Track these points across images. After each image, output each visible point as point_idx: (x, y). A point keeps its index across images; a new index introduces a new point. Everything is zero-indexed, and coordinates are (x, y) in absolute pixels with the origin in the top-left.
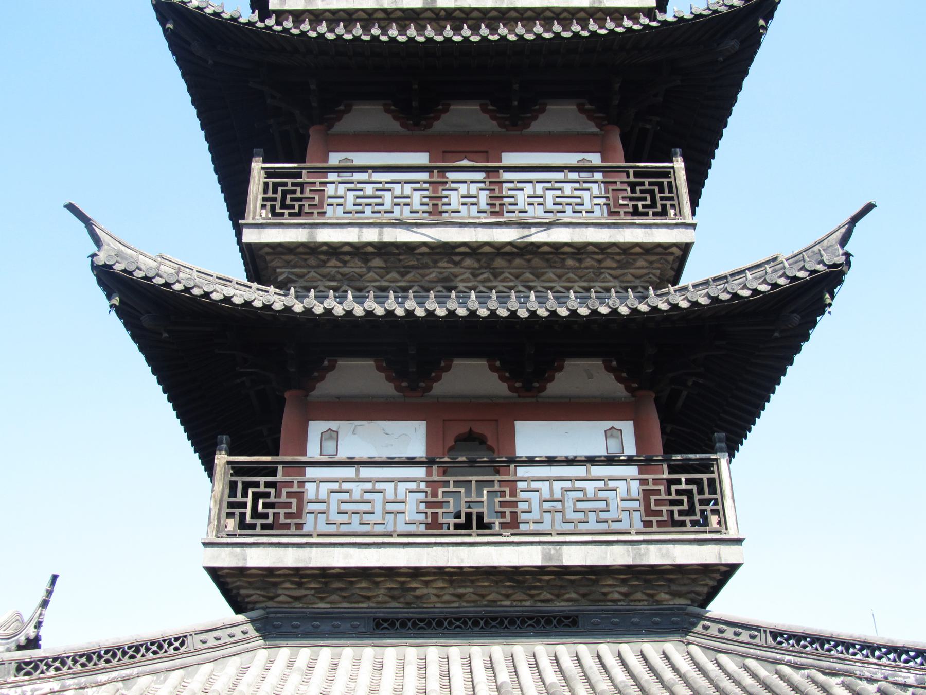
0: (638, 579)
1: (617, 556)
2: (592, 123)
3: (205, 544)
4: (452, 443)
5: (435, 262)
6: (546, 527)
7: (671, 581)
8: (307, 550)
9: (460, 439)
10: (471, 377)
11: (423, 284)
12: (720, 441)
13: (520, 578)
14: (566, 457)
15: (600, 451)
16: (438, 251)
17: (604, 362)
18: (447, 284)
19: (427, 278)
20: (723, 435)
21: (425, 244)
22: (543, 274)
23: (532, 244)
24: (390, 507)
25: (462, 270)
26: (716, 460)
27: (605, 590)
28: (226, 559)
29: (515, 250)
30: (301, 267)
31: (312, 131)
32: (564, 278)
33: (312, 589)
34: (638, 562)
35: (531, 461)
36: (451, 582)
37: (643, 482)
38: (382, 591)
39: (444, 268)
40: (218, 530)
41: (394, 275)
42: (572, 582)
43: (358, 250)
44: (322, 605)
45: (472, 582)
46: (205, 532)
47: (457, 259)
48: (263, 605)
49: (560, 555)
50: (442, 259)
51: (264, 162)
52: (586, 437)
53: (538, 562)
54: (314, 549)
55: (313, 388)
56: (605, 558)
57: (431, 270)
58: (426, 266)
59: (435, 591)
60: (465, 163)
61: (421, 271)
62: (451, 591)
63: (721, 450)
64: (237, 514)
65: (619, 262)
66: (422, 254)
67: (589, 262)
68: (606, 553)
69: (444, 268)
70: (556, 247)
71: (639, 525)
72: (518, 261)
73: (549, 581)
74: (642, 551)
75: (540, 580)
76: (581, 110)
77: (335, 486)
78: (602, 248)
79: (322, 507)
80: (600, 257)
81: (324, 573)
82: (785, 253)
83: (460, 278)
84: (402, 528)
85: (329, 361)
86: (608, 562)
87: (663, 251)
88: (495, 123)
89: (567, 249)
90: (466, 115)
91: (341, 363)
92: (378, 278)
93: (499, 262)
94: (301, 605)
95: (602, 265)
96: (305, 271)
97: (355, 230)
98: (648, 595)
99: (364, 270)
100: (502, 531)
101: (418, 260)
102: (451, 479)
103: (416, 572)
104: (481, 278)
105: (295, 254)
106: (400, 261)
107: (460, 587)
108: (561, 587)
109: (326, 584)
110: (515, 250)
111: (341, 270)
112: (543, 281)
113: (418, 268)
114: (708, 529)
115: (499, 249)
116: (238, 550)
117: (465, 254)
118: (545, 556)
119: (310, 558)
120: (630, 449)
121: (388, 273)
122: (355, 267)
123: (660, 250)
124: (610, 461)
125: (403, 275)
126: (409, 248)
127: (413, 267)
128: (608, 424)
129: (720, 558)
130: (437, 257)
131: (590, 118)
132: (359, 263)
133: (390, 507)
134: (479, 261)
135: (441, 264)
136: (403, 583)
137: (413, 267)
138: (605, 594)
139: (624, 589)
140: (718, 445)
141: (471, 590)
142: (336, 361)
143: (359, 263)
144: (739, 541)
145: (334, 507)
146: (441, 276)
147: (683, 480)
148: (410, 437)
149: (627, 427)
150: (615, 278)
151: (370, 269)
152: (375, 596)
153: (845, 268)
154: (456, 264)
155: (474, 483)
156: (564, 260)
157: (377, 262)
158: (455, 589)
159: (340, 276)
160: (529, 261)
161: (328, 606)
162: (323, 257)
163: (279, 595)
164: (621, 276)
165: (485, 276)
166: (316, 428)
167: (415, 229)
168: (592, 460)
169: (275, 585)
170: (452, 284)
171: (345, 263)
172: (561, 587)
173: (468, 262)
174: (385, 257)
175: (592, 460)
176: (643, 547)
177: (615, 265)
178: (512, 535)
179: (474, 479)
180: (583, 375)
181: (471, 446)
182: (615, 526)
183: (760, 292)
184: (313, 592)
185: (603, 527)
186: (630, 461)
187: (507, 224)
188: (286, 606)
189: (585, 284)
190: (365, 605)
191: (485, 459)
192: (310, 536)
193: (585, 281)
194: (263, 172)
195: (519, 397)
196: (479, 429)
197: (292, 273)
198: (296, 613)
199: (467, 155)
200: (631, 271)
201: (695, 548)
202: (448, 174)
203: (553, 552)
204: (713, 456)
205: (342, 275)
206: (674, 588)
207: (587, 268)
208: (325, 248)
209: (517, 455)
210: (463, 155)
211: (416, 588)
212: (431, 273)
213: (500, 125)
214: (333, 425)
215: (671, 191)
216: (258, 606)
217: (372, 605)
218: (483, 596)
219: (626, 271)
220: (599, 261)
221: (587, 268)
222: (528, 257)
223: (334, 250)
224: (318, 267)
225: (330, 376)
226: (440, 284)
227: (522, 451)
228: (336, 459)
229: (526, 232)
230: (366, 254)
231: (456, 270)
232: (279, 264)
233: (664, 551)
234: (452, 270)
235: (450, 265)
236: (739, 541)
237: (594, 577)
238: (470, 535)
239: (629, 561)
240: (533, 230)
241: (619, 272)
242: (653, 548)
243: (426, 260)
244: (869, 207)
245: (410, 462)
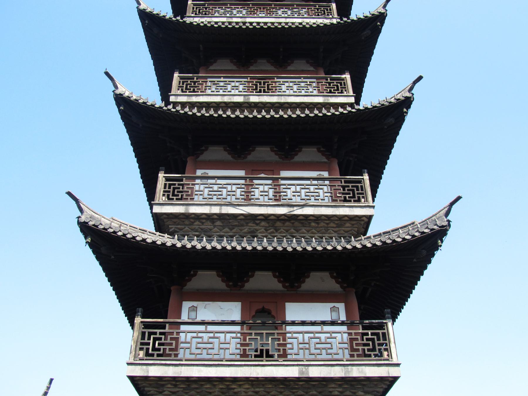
0: (347, 384)
1: (337, 372)
2: (324, 157)
3: (128, 364)
5: (247, 223)
6: (300, 357)
7: (364, 385)
9: (258, 312)
10: (264, 281)
11: (241, 234)
12: (388, 313)
13: (288, 383)
14: (311, 321)
15: (328, 318)
17: (330, 273)
18: (253, 234)
19: (243, 231)
20: (389, 310)
21: (242, 214)
22: (300, 230)
23: (295, 215)
24: (222, 346)
25: (260, 228)
26: (386, 323)
27: (331, 390)
28: (138, 371)
29: (286, 218)
30: (181, 225)
31: (188, 159)
33: (181, 388)
34: (347, 375)
35: (293, 323)
36: (252, 385)
37: (350, 334)
38: (217, 390)
40: (135, 357)
41: (227, 229)
42: (314, 385)
43: (209, 217)
45: (263, 385)
46: (128, 357)
47: (258, 222)
49: (308, 373)
51: (165, 173)
52: (321, 311)
53: (296, 375)
54: (183, 367)
55: (186, 285)
56: (331, 373)
58: (242, 225)
59: (244, 390)
60: (263, 175)
61: (240, 228)
62: (253, 390)
63: (389, 318)
64: (145, 348)
65: (337, 224)
66: (241, 219)
67: (322, 224)
68: (331, 371)
70: (306, 217)
71: (347, 356)
72: (287, 224)
73: (302, 385)
74: (349, 370)
75: (297, 385)
76: (319, 151)
77: (195, 335)
78: (329, 217)
79: (188, 345)
80: (328, 222)
81: (188, 380)
82: (418, 220)
83: (259, 231)
84: (228, 357)
85: (194, 272)
86: (332, 375)
87: (359, 219)
88: (277, 156)
89: (311, 218)
90: (263, 153)
91: (200, 273)
92: (219, 231)
93: (278, 224)
95: (329, 226)
96: (183, 227)
97: (208, 207)
98: (352, 392)
100: (278, 359)
101: (239, 222)
102: (253, 332)
103: (235, 380)
104: (269, 231)
105: (179, 219)
106: (230, 222)
107: (257, 388)
108: (309, 388)
109: (189, 385)
110: (286, 218)
111: (201, 227)
112: (300, 233)
113: (239, 226)
114: (382, 358)
115: (278, 217)
116: (144, 367)
118: (301, 372)
119: (181, 372)
120: (343, 317)
121: (224, 229)
122: (208, 225)
123: (357, 218)
124: (333, 323)
125: (231, 230)
126: (234, 216)
128: (332, 305)
129: (389, 373)
130: (247, 221)
131: (323, 155)
132: (210, 224)
133: (222, 346)
134: (268, 223)
135: (250, 224)
136: (229, 385)
137: (236, 226)
138: (331, 392)
139: (340, 390)
140: (387, 315)
141: (263, 389)
142: (197, 272)
143: (209, 223)
144: (398, 365)
145: (194, 346)
146: (250, 230)
147: (370, 333)
148: (233, 311)
149: (341, 306)
150: (335, 232)
151: (215, 226)
153: (448, 228)
154: (257, 224)
155: (264, 334)
156: (310, 223)
157: (218, 223)
158: (254, 389)
159: (200, 230)
160: (293, 223)
162: (192, 220)
163: (165, 391)
165: (271, 230)
166: (186, 305)
167: (237, 207)
168: (324, 323)
169: (163, 386)
170: (255, 234)
171: (203, 223)
172: (309, 388)
173: (263, 223)
175: (324, 323)
176: (350, 367)
177: (335, 226)
178: (284, 361)
179: (264, 332)
180: (319, 280)
181: (264, 315)
182: (335, 357)
183: (406, 239)
184: (182, 389)
185: (330, 357)
186: (343, 323)
187: (282, 205)
189: (321, 235)
191: (270, 322)
192: (181, 360)
194: (164, 178)
195: (288, 290)
196: (268, 306)
197: (177, 228)
200: (343, 229)
201: (376, 368)
202: (254, 181)
203: (304, 370)
204: (384, 321)
205: (202, 229)
206: (366, 389)
207: (321, 227)
208: (193, 216)
209: (287, 320)
210: (262, 172)
211: (235, 388)
213: (280, 158)
214: (195, 304)
215: (362, 190)
218: (268, 393)
220: (328, 224)
221: (321, 227)
222: (292, 221)
223: (198, 217)
224: (190, 225)
225: (194, 279)
227: (289, 318)
228: (196, 321)
229: (291, 209)
230: (213, 219)
231: (257, 227)
232: (171, 223)
233: (360, 370)
234: (255, 228)
235: (254, 225)
236: (398, 365)
237: (325, 383)
238: (262, 361)
239: (342, 375)
240: (295, 208)
241: (337, 229)
242: (354, 368)
243: (242, 222)
244: (459, 198)
245: (233, 323)
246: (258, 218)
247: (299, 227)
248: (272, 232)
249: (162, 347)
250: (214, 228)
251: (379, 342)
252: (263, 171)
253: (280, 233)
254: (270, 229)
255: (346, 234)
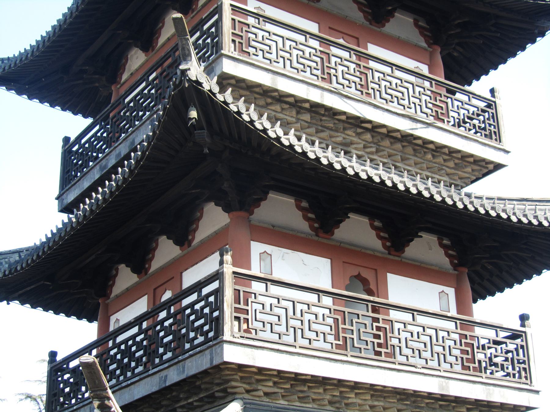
2: (422, 39)
4: (348, 282)
5: (345, 129)
8: (296, 357)
10: (357, 230)
16: (350, 121)
17: (438, 239)
18: (345, 148)
19: (333, 139)
21: (344, 113)
22: (408, 159)
32: (418, 166)
38: (328, 397)
39: (348, 135)
44: (282, 402)
45: (385, 397)
47: (359, 130)
48: (241, 396)
50: (351, 128)
57: (339, 134)
58: (337, 131)
62: (370, 403)
67: (440, 160)
69: (348, 135)
73: (427, 403)
76: (416, 24)
78: (452, 152)
81: (297, 379)
88: (361, 14)
93: (386, 142)
94: (268, 400)
95: (445, 164)
97: (269, 76)
99: (294, 120)
101: (334, 124)
103: (356, 386)
105: (252, 92)
106: (321, 120)
112: (405, 164)
113: (331, 129)
117: (366, 129)
121: (309, 127)
127: (328, 128)
128: (441, 288)
129: (529, 403)
131: (422, 34)
135: (349, 132)
137: (328, 128)
141: (381, 404)
142: (268, 193)
144: (537, 392)
150: (448, 174)
151: (298, 120)
152: (319, 400)
154: (358, 134)
156: (425, 153)
157: (307, 117)
158: (373, 401)
161: (286, 403)
163: (257, 390)
164: (451, 174)
173: (368, 136)
174: (313, 115)
188: (258, 399)
190: (310, 406)
193: (430, 172)
195: (389, 254)
196: (365, 274)
198: (264, 406)
199: (345, 36)
200: (460, 173)
202: (370, 62)
203: (444, 384)
210: (342, 35)
212: (337, 136)
213: (366, 18)
216: (237, 396)
217: (316, 406)
219: (457, 172)
226: (340, 147)
230: (301, 108)
231: (355, 139)
236: (537, 392)
240: (419, 125)
241: (453, 171)
243: (341, 126)
246: (364, 125)
247: (410, 155)
248: (371, 153)
249: (341, 335)
250: (296, 123)
251: (344, 326)
252: (344, 34)
253: (380, 157)
254: (371, 147)
255: (459, 182)
